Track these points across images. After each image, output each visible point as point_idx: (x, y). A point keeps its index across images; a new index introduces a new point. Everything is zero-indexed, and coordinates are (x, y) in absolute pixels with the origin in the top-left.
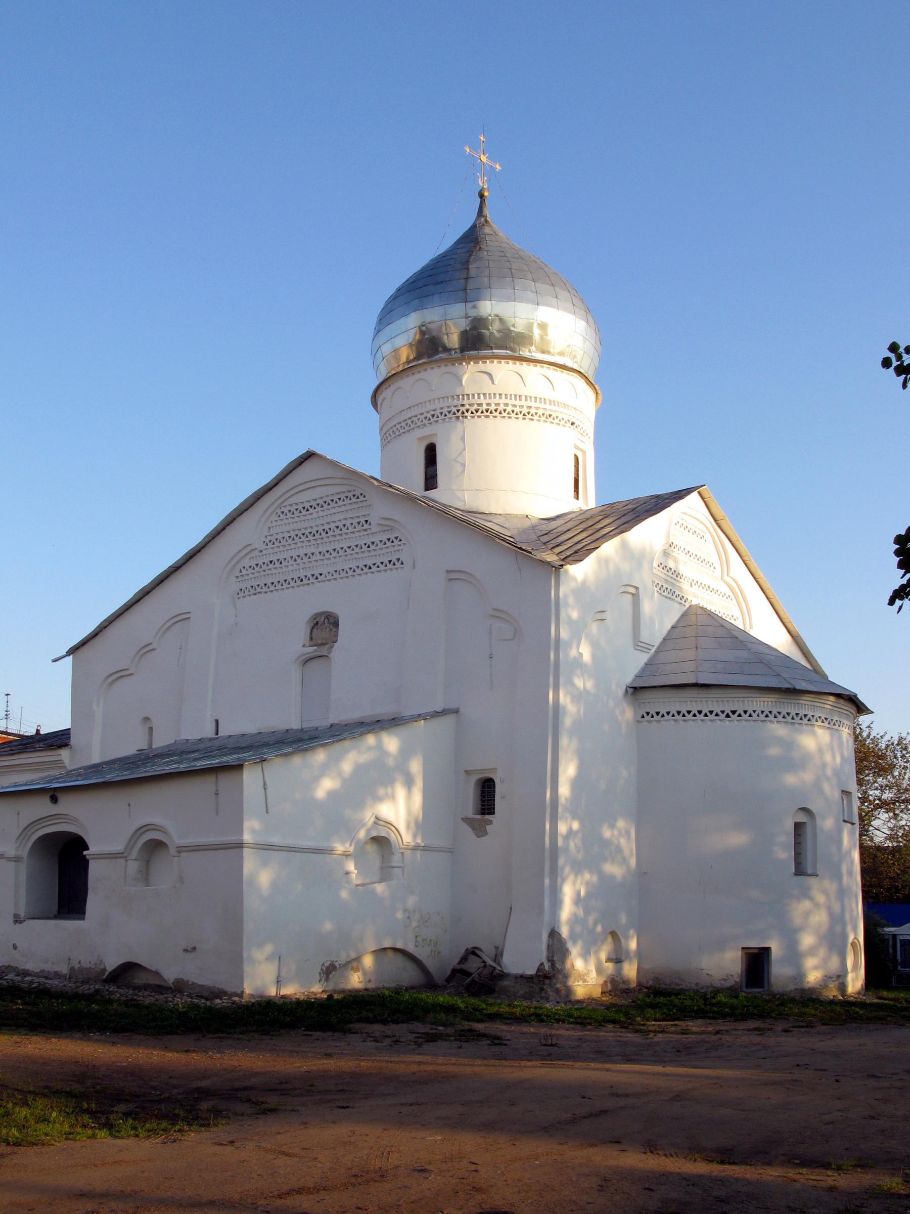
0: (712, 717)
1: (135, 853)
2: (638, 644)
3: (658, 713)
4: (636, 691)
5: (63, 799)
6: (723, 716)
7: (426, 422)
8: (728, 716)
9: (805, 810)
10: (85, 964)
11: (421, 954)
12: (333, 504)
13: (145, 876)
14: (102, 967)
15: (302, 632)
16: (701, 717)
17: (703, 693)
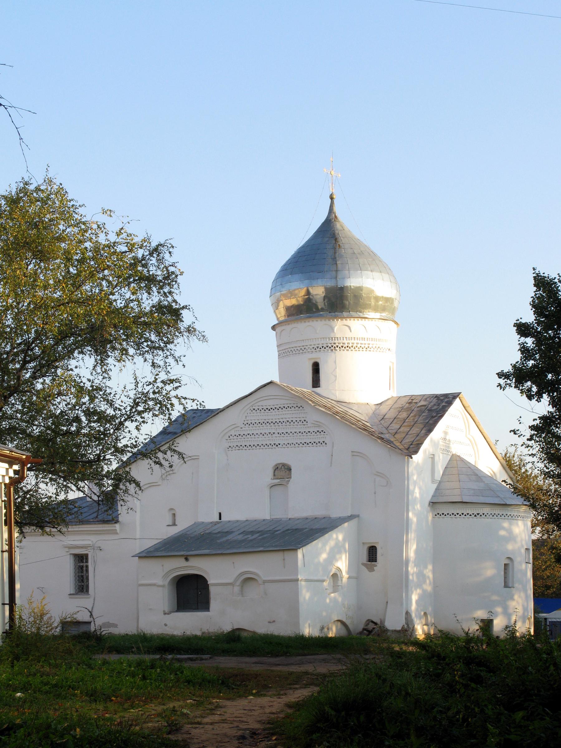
0: (468, 516)
1: (238, 583)
2: (433, 481)
3: (443, 514)
4: (433, 504)
6: (473, 516)
7: (314, 350)
8: (475, 516)
9: (508, 558)
12: (284, 409)
13: (242, 593)
14: (222, 631)
16: (463, 516)
17: (464, 505)
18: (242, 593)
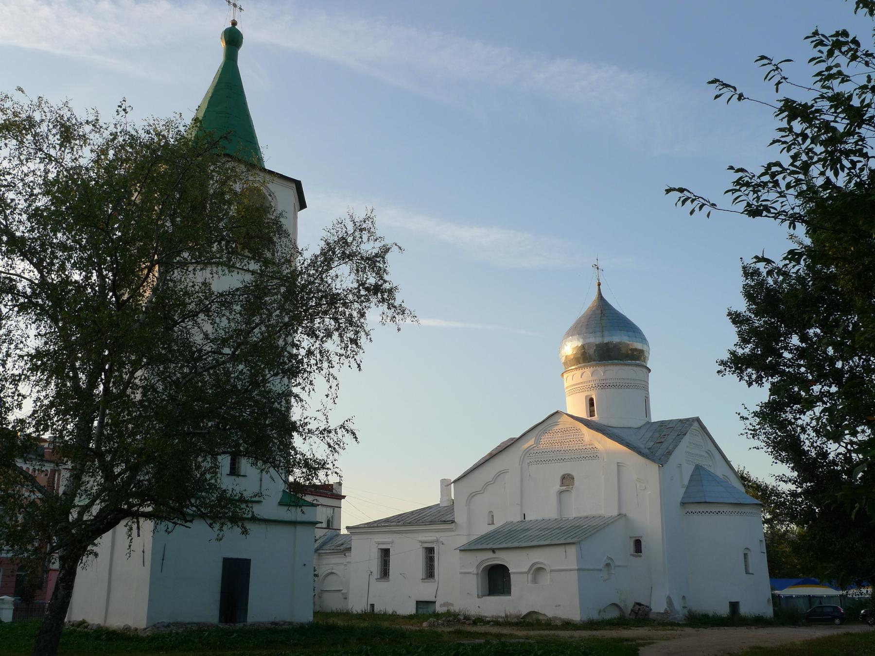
4: (683, 504)
5: (497, 552)
10: (512, 612)
11: (622, 605)
13: (535, 581)
15: (559, 481)
18: (535, 581)
